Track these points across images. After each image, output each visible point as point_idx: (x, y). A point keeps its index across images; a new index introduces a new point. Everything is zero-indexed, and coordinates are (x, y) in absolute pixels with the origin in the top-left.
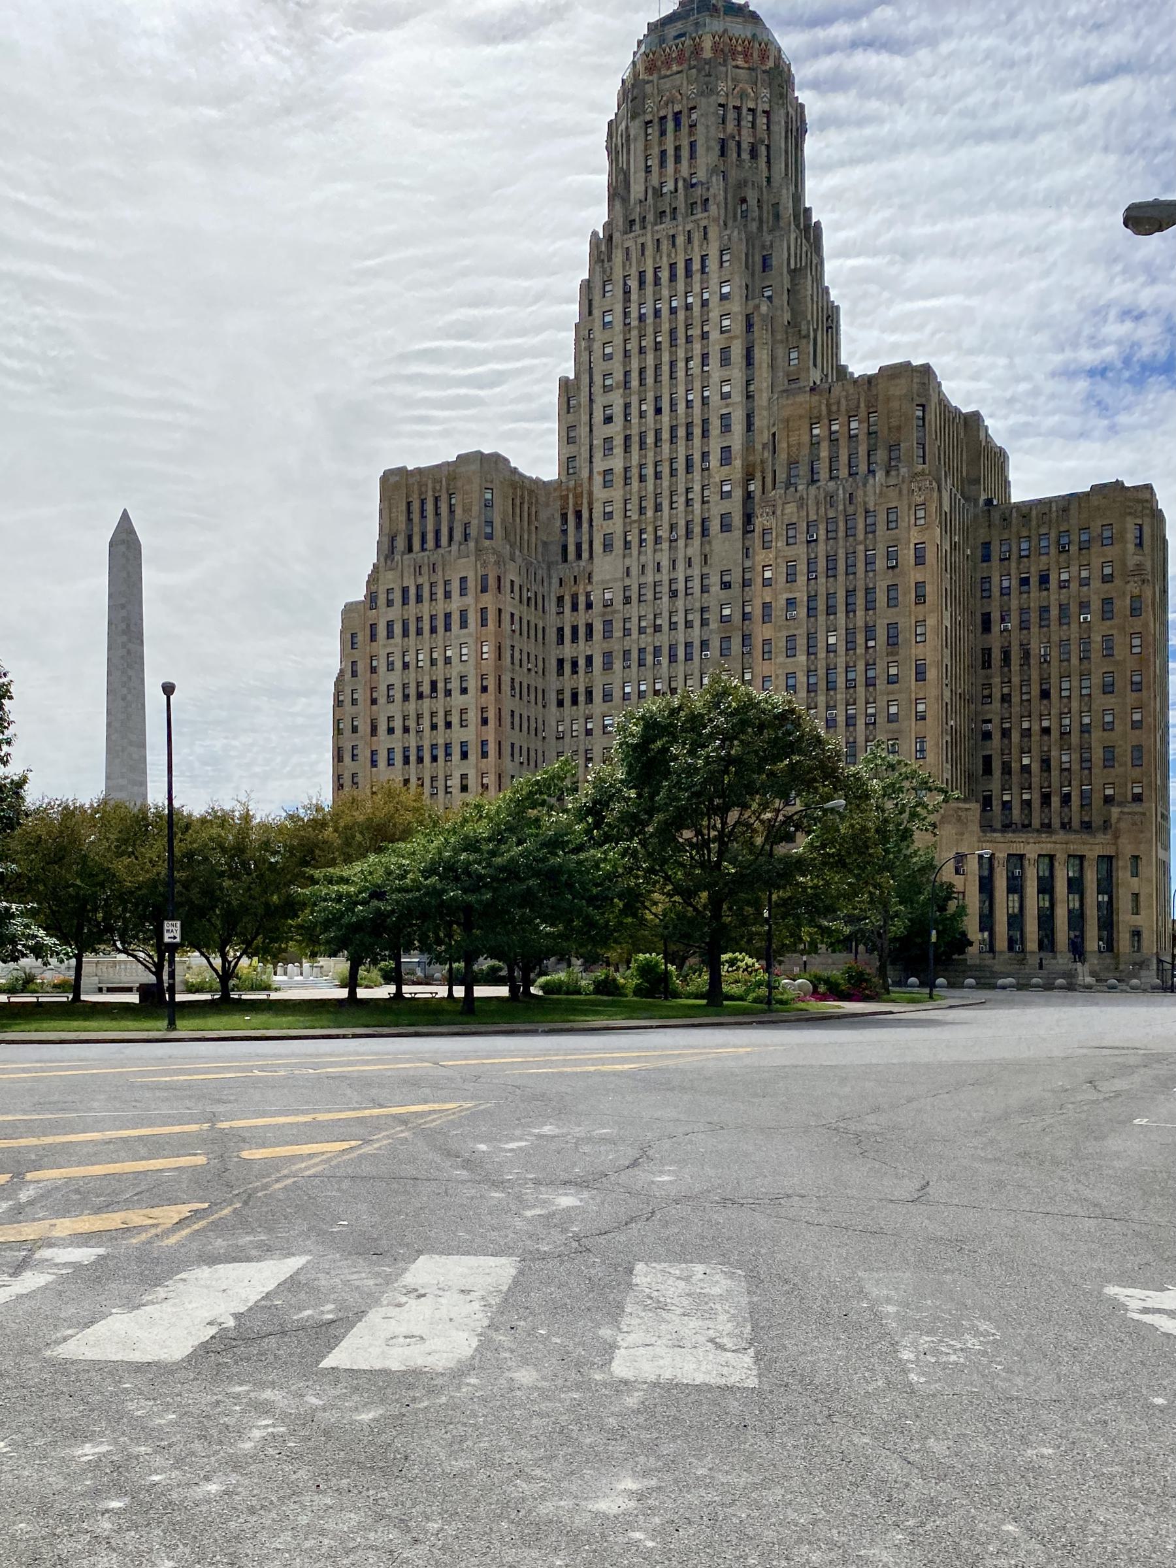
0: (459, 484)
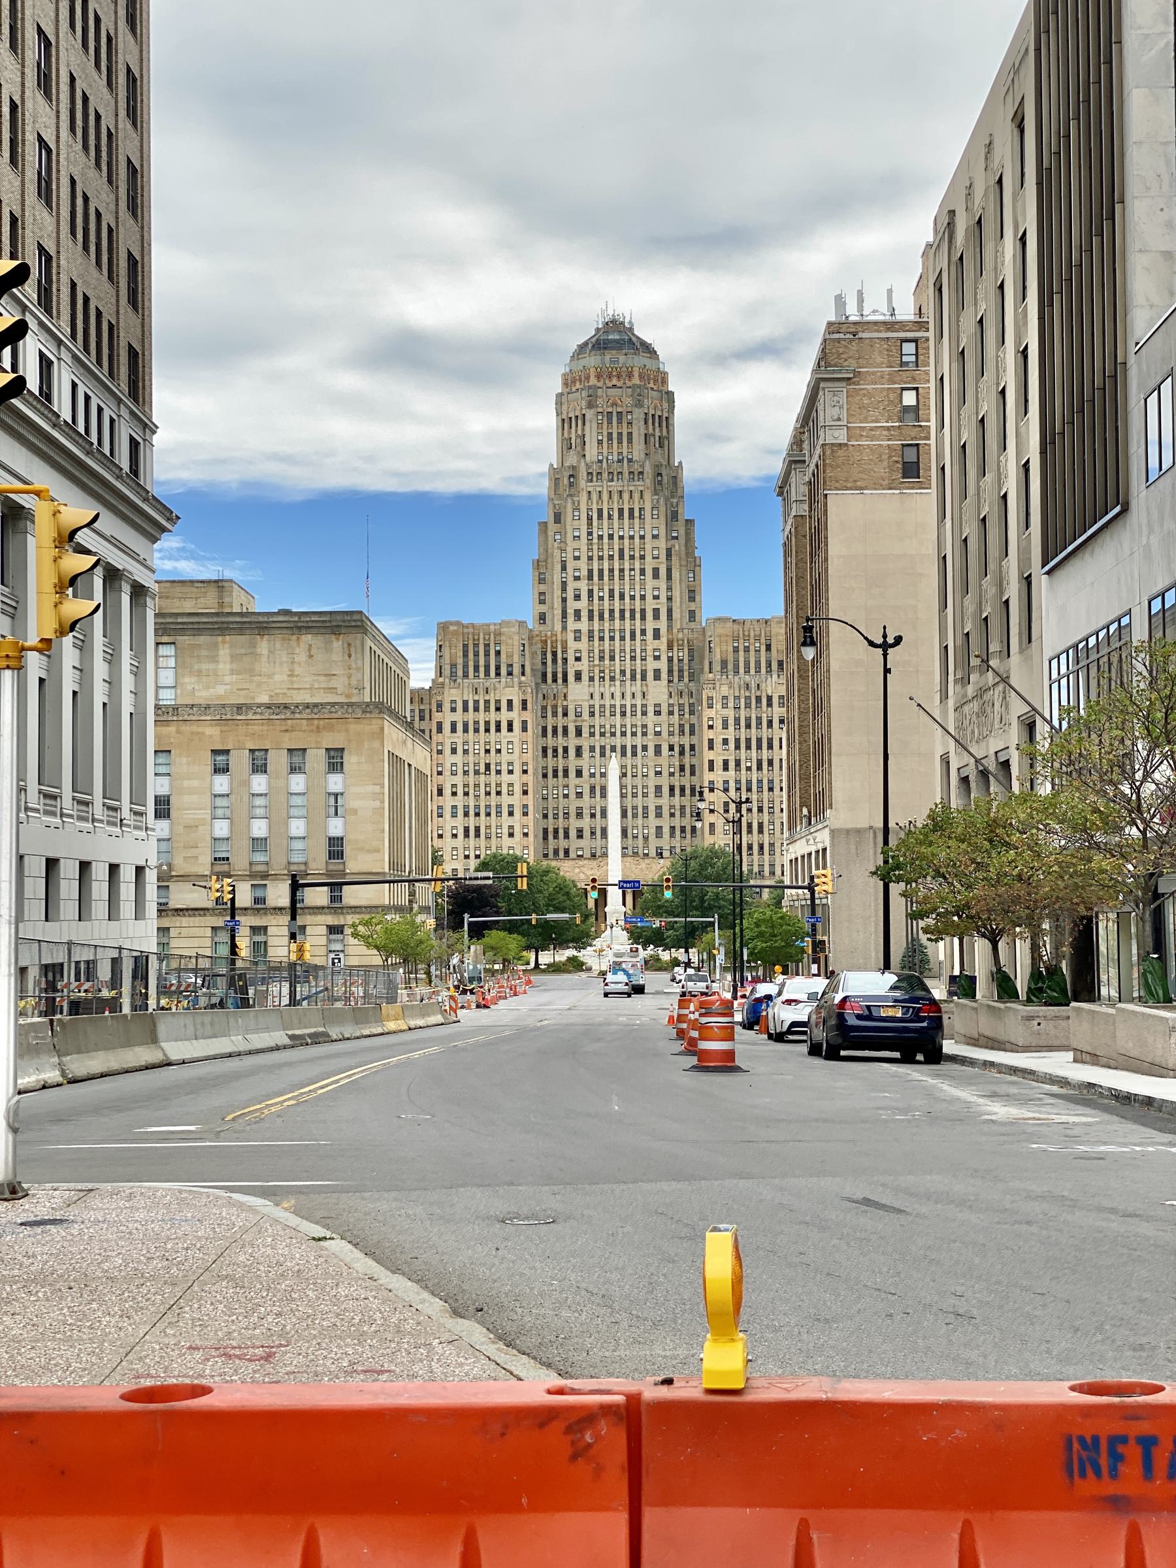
0: (503, 638)
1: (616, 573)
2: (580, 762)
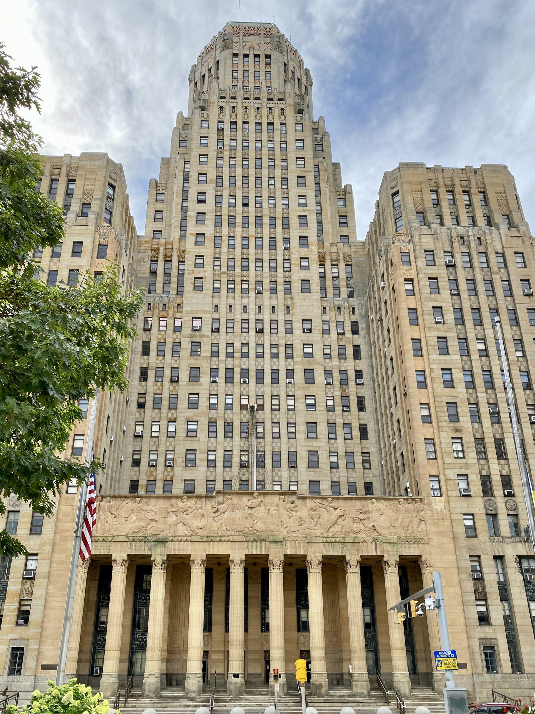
1: (252, 179)
2: (195, 389)
